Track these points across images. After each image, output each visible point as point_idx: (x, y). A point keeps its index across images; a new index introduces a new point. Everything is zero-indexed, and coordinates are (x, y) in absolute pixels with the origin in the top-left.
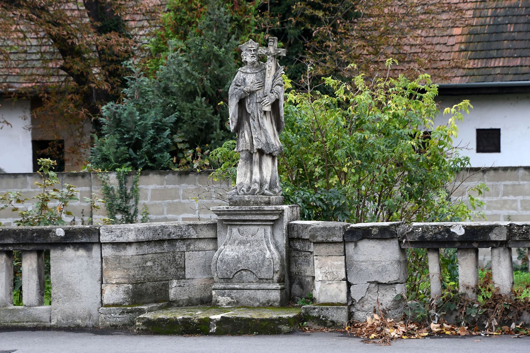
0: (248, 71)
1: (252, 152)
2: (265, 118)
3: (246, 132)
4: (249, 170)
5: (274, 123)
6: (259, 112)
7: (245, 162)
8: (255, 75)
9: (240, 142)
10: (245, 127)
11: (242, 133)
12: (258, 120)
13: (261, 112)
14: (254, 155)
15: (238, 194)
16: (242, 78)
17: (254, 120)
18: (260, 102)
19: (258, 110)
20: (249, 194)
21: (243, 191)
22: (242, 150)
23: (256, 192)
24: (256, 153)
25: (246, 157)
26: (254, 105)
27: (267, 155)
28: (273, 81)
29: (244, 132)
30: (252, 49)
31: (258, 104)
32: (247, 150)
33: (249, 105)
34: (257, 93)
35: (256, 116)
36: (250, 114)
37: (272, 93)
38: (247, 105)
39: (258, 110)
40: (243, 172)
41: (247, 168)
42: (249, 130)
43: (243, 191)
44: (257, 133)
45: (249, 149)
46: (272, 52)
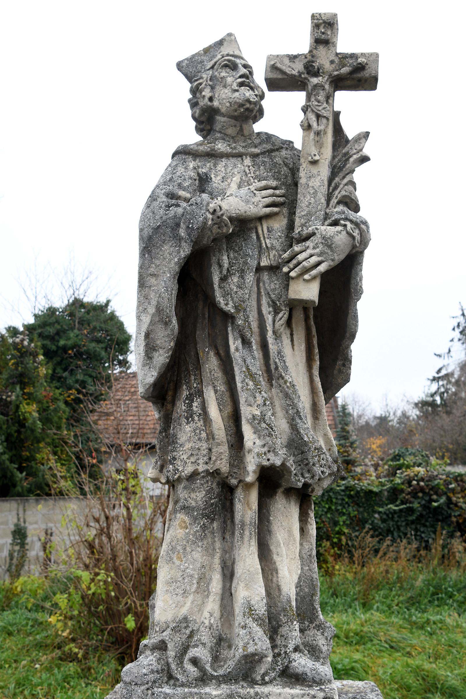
0: (221, 146)
1: (234, 482)
2: (286, 341)
3: (210, 396)
4: (217, 561)
5: (317, 364)
6: (266, 309)
7: (204, 528)
8: (248, 161)
9: (182, 438)
10: (206, 375)
11: (190, 399)
12: (264, 346)
13: (276, 311)
14: (239, 494)
15: (170, 677)
16: (192, 174)
17: (246, 342)
18: (274, 269)
19: (264, 301)
20: (227, 679)
21: (195, 661)
22: (194, 475)
23: (262, 669)
24: (248, 486)
25: (208, 504)
26: (250, 278)
27: (289, 492)
28: (330, 180)
29: (200, 393)
30: (238, 61)
31: (265, 276)
32: (217, 472)
33: (223, 279)
34: (264, 228)
35: (254, 325)
36: (228, 317)
37: (335, 223)
38: (216, 279)
39: (264, 301)
40: (193, 570)
41: (210, 551)
42: (222, 387)
43: (195, 661)
44: (260, 400)
45: (225, 468)
46: (328, 67)
